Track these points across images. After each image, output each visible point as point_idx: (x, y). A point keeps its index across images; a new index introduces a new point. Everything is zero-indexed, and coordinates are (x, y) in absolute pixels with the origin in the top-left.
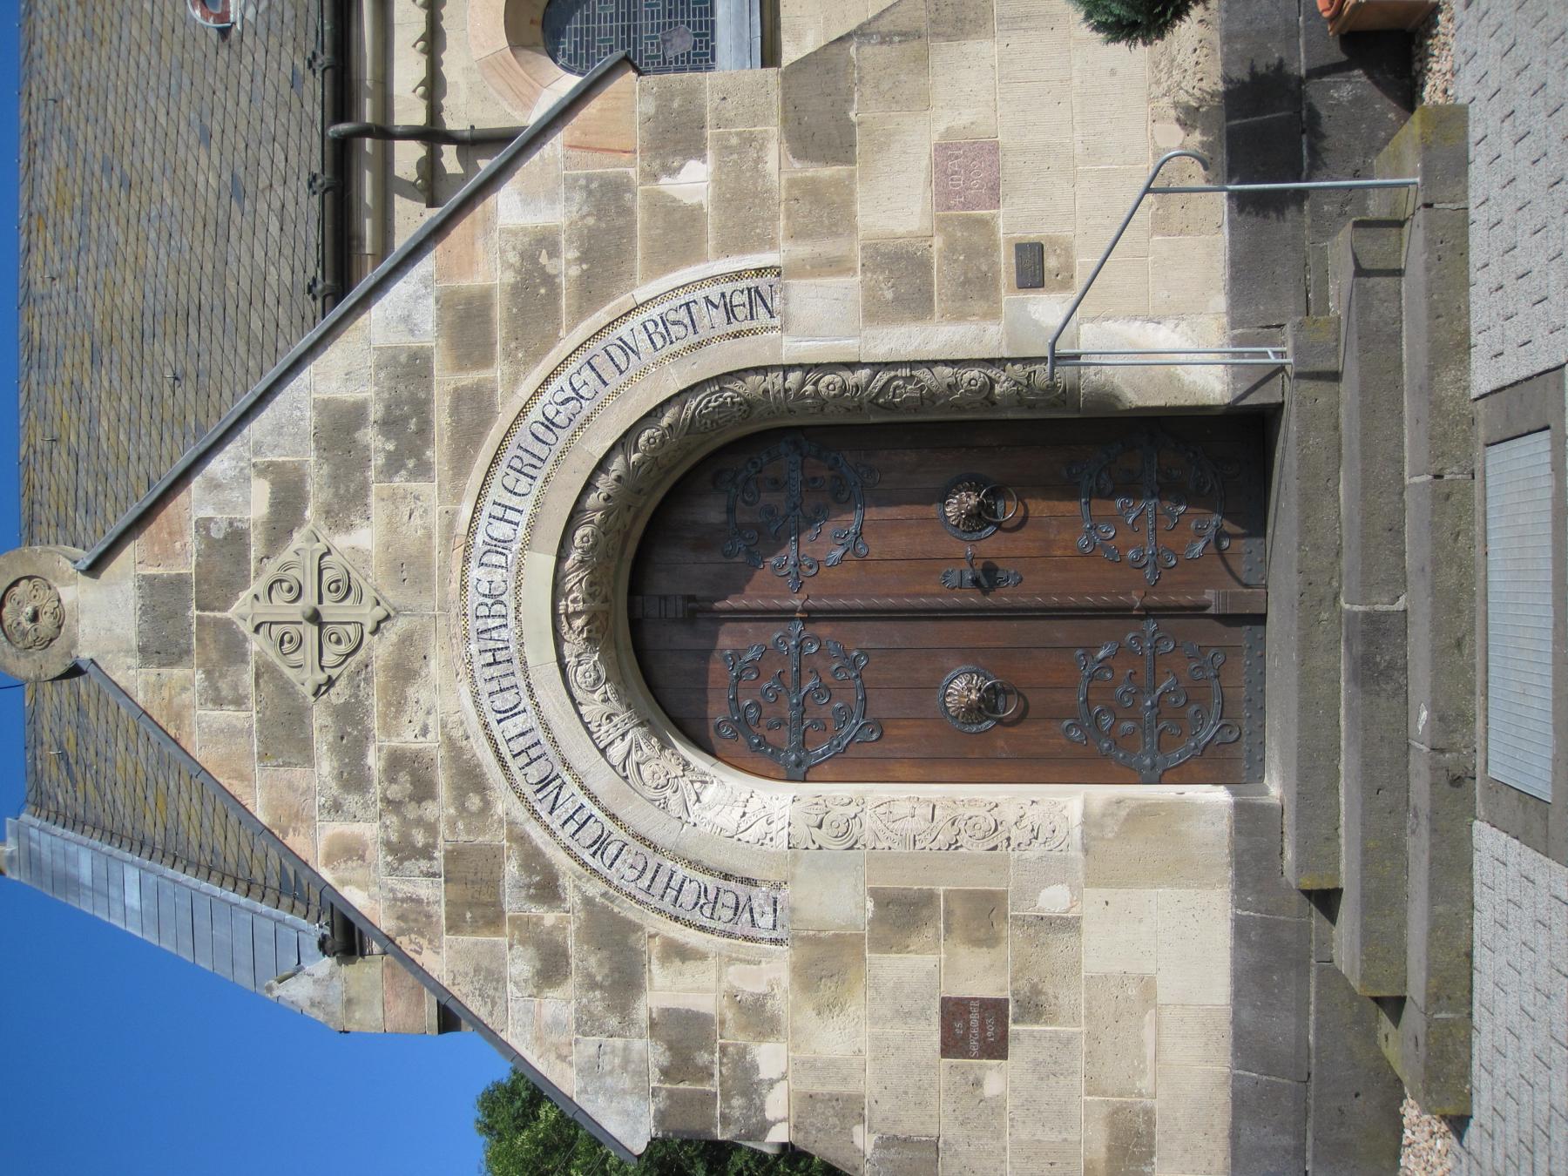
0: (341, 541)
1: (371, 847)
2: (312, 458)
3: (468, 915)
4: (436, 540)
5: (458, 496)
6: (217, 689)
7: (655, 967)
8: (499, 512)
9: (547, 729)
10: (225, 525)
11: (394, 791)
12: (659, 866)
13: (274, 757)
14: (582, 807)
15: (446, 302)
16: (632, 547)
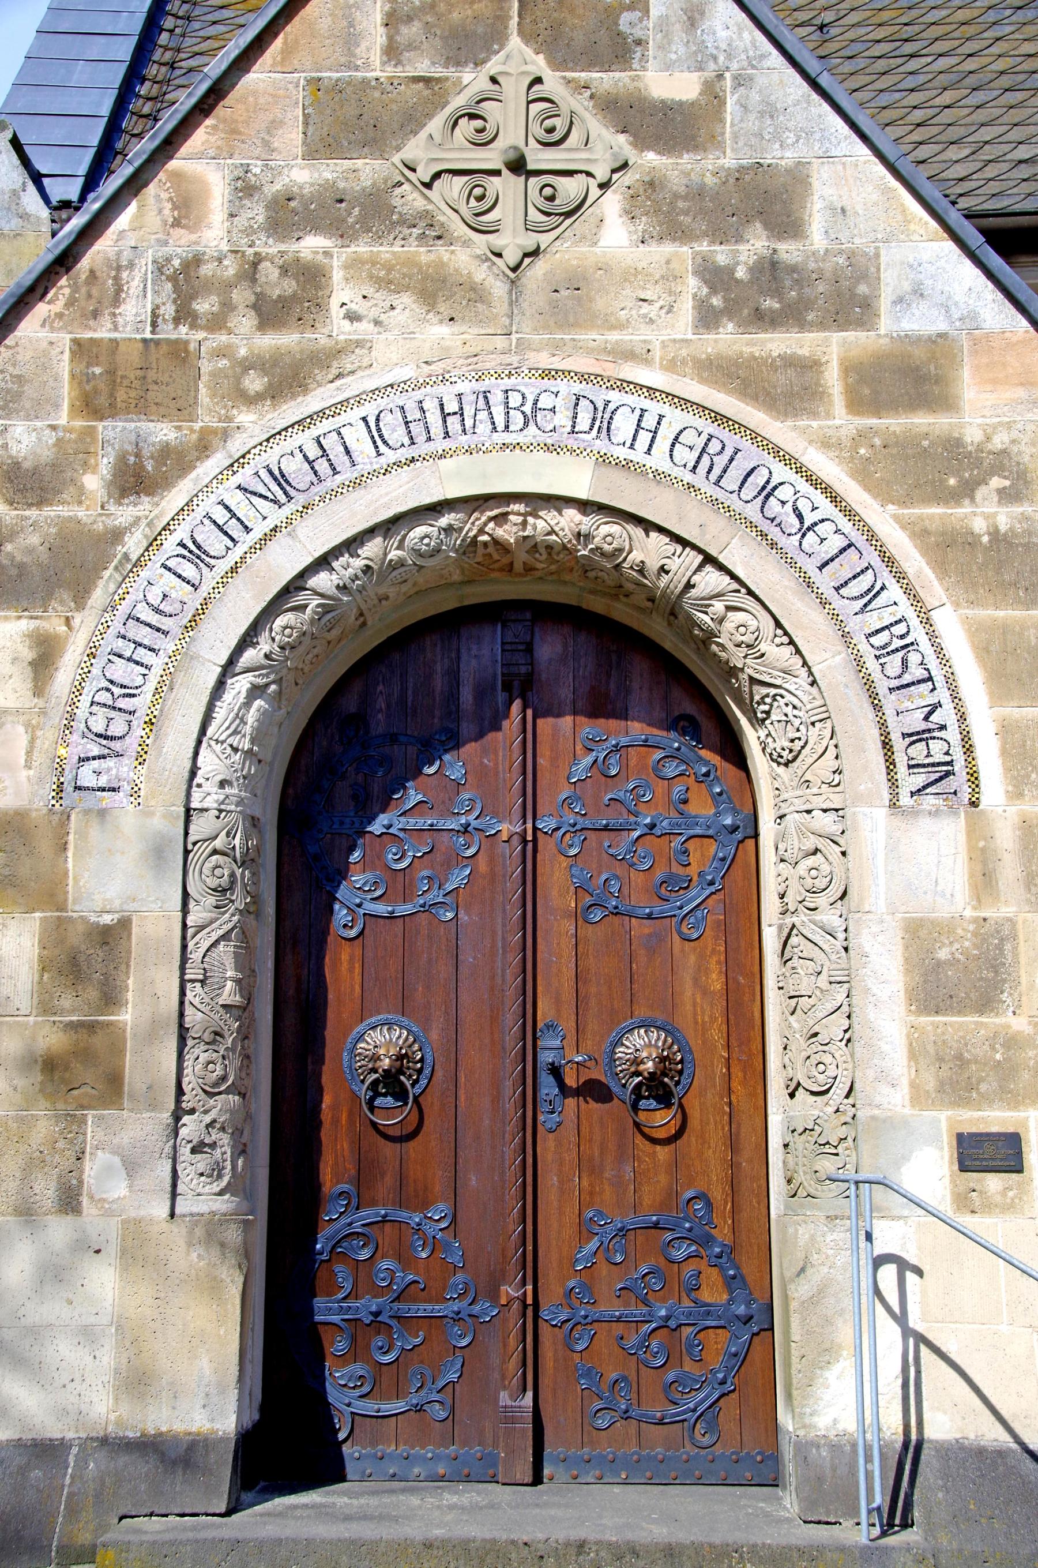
0: (612, 204)
1: (193, 237)
2: (729, 161)
3: (98, 370)
4: (614, 336)
5: (671, 366)
6: (409, 19)
7: (25, 625)
8: (649, 422)
9: (357, 483)
10: (638, 33)
11: (269, 272)
12: (166, 633)
13: (316, 103)
14: (247, 529)
16: (597, 605)
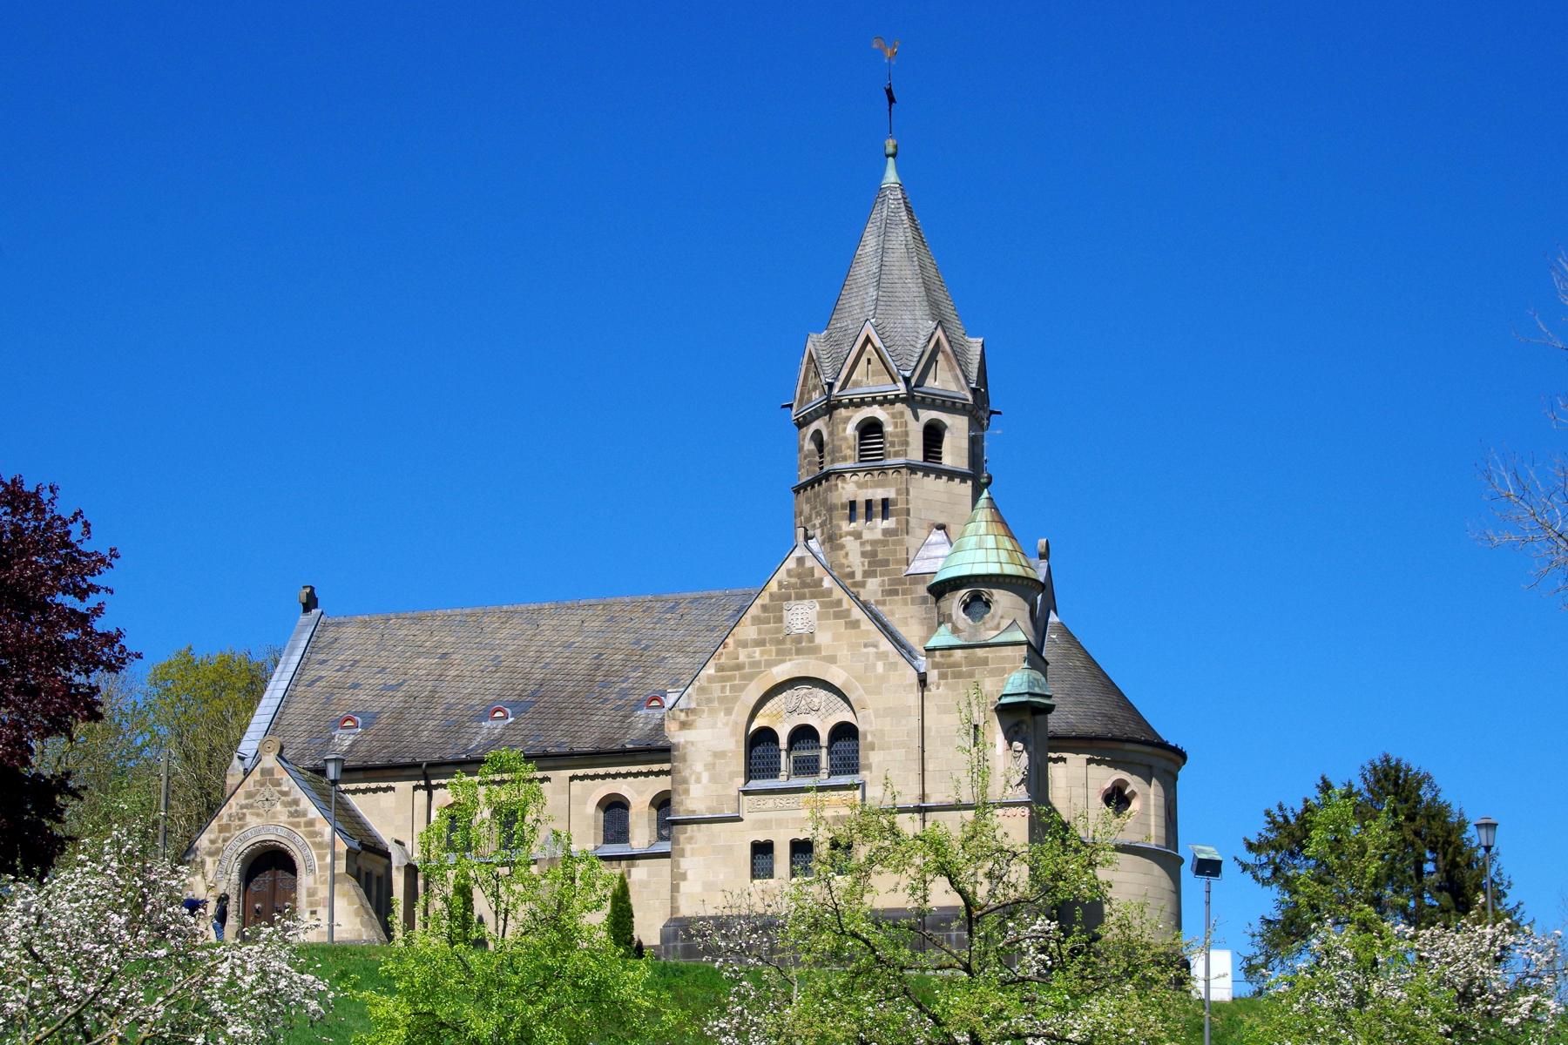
0: (278, 803)
2: (292, 797)
5: (285, 823)
15: (314, 819)
